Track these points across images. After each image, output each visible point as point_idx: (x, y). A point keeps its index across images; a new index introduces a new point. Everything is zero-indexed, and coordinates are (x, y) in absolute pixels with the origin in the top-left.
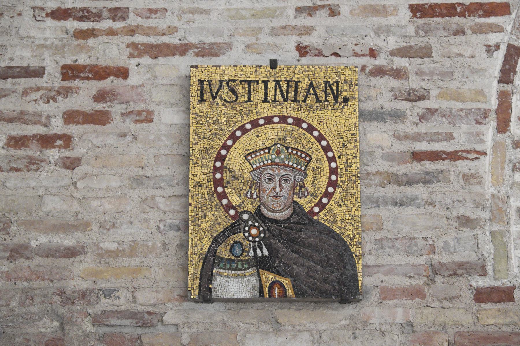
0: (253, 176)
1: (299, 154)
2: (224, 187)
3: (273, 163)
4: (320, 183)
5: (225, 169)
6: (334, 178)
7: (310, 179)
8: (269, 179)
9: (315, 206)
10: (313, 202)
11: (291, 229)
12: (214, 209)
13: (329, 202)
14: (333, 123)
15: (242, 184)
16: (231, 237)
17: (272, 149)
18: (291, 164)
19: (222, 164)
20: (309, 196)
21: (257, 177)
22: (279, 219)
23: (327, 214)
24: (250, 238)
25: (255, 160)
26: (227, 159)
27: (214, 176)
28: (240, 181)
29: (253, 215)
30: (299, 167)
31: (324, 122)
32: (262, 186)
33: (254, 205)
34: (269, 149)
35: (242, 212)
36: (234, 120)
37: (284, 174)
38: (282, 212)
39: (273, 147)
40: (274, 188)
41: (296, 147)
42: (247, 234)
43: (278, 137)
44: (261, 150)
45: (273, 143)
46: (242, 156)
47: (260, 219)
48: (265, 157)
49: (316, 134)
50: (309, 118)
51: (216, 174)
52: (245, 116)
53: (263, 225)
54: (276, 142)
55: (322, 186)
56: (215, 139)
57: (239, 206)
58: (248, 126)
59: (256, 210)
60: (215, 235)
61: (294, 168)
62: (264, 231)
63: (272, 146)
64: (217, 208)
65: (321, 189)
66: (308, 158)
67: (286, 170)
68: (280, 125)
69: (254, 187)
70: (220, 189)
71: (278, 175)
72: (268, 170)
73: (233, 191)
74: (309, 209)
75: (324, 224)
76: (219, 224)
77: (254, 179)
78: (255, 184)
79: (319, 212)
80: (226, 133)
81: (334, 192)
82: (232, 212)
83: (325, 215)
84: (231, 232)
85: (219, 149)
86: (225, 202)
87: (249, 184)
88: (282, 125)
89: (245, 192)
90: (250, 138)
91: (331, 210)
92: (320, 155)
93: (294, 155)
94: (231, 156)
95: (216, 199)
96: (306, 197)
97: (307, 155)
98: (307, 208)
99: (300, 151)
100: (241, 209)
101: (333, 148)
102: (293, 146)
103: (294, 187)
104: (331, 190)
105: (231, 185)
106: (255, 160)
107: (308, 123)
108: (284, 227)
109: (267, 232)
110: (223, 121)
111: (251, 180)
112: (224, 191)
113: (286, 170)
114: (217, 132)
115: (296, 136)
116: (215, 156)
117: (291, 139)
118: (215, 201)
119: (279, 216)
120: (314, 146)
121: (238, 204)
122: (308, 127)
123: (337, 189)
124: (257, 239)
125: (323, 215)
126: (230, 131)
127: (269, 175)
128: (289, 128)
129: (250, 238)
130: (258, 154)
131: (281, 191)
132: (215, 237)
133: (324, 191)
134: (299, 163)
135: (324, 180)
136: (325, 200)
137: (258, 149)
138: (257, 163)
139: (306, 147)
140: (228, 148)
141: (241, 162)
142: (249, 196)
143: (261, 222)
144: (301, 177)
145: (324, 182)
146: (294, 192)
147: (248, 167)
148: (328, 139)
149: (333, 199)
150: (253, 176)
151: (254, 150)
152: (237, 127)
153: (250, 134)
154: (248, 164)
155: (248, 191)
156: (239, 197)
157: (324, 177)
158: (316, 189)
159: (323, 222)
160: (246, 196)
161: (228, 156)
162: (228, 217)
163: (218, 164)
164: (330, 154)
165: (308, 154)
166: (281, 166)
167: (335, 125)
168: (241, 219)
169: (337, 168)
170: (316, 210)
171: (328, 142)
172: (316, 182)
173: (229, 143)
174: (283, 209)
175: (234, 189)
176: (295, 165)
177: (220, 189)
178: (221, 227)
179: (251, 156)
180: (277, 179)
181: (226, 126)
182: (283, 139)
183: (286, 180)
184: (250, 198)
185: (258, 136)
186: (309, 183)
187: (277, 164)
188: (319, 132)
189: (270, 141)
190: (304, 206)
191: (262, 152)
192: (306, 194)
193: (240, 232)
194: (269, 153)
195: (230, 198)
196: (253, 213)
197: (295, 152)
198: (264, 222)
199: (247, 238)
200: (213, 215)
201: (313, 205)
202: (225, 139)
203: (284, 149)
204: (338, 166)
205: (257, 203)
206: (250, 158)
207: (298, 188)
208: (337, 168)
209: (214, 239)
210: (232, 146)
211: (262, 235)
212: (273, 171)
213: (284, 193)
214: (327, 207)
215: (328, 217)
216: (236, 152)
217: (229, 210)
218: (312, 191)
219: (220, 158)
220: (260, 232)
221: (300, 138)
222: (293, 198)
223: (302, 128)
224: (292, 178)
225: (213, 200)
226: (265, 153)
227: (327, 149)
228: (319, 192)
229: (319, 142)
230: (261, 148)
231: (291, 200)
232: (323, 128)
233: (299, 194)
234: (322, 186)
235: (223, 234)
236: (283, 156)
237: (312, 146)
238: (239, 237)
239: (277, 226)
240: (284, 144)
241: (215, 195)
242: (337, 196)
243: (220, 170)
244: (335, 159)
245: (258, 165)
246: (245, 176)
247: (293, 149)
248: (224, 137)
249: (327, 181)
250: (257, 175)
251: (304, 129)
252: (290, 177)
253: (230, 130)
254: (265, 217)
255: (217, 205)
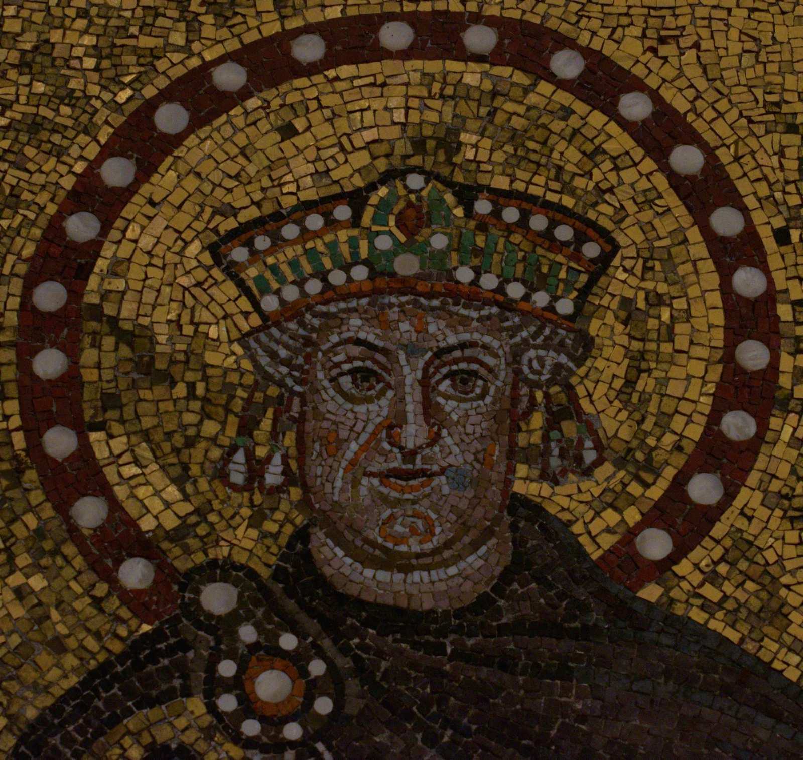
0: (264, 360)
1: (538, 222)
2: (82, 429)
3: (381, 283)
4: (674, 389)
5: (93, 325)
6: (753, 355)
7: (609, 363)
8: (362, 375)
9: (648, 521)
10: (633, 501)
11: (503, 667)
12: (23, 560)
13: (729, 496)
14: (735, 48)
15: (196, 405)
16: (131, 723)
17: (374, 199)
18: (489, 282)
19: (75, 293)
20: (607, 468)
21: (287, 363)
22: (427, 604)
23: (723, 569)
24: (251, 728)
25: (274, 269)
26: (101, 264)
27: (24, 364)
28: (181, 390)
29: (262, 587)
30: (541, 299)
31: (685, 42)
32: (319, 416)
33: (271, 527)
34: (357, 199)
35: (199, 569)
36: (146, 42)
37: (452, 340)
38: (445, 564)
39: (383, 191)
40: (393, 425)
41: (520, 186)
42: (228, 703)
43: (410, 132)
44: (308, 206)
45: (382, 165)
46: (194, 249)
47: (312, 613)
48: (333, 246)
49: (635, 107)
50: (595, 24)
51: (35, 352)
52: (209, 19)
53: (326, 643)
54: (396, 161)
55: (685, 407)
56: (30, 152)
57: (177, 535)
58: (230, 77)
59: (283, 558)
60: (31, 713)
61: (508, 306)
62: (334, 683)
63: (372, 187)
64: (43, 552)
65: (678, 423)
66: (592, 247)
67: (465, 321)
68: (418, 64)
69: (266, 424)
70: (59, 442)
71: (412, 350)
72: (355, 321)
73: (143, 450)
74: (607, 541)
75: (702, 631)
76: (58, 646)
77: (268, 377)
78: (278, 403)
79: (674, 558)
80: (99, 119)
81: (760, 438)
82: (135, 573)
83: (712, 578)
84: (128, 692)
85: (52, 209)
86: (89, 512)
87: (238, 405)
88: (433, 66)
89: (216, 453)
90: (241, 140)
91: (742, 547)
92: (664, 226)
93: (509, 229)
94: (125, 250)
95: (36, 497)
96: (587, 472)
97: (587, 229)
98: (597, 534)
99: (547, 206)
100: (188, 551)
101: (743, 186)
102: (501, 182)
103: (511, 417)
104: (738, 425)
105: (128, 413)
106: (274, 269)
107: (587, 52)
108: (459, 655)
109: (353, 686)
110: (78, 52)
111: (249, 380)
112: (85, 450)
113: (465, 321)
114: (44, 111)
115: (518, 123)
116: (29, 250)
117: (487, 143)
118: (30, 509)
119: (424, 589)
120: (629, 175)
121: (170, 522)
122: (589, 70)
123: (774, 423)
124: (292, 732)
125: (697, 578)
126: (118, 108)
127: (356, 350)
128: (471, 79)
129: (251, 728)
130: (290, 231)
131: (435, 439)
132: (32, 726)
133: (695, 432)
134: (544, 277)
135: (697, 368)
136: (703, 489)
137: (289, 202)
138: (282, 281)
139: (580, 182)
140: (107, 204)
141: (185, 281)
142: (238, 478)
143: (312, 625)
144: (551, 357)
145: (696, 384)
146: (513, 444)
147: (231, 308)
148: (708, 137)
149: (753, 478)
150: (264, 360)
151: (268, 208)
152: (162, 83)
153: (240, 122)
154: (231, 289)
155: (234, 449)
156: (179, 482)
157: (697, 351)
158: (648, 425)
159: (697, 616)
160: (222, 475)
161: (108, 250)
162: (114, 603)
163: (50, 296)
164: (726, 222)
165: (593, 225)
166: (430, 296)
167: (748, 60)
168: (194, 611)
169: (771, 296)
170: (656, 545)
171: (709, 152)
172: (645, 383)
173: (117, 172)
174: (447, 545)
175: (146, 436)
176: (515, 291)
177: (59, 442)
178: (70, 661)
179: (249, 244)
180: (410, 374)
181: (95, 77)
182: (441, 143)
183: (463, 380)
184: (248, 487)
185: (288, 132)
186: (602, 388)
187: (405, 286)
188: (655, 96)
189: (361, 159)
190: (577, 528)
191: (315, 221)
192: (590, 456)
193: (187, 693)
194: (355, 221)
195: (121, 492)
196: (265, 573)
197: (511, 215)
198: (330, 627)
199: (225, 727)
200: (20, 593)
201: (633, 516)
202: (92, 151)
203: (449, 198)
204: (780, 284)
205: (285, 517)
206: (240, 254)
207: (537, 420)
208: (771, 296)
209: (21, 740)
210: (130, 191)
211: (324, 706)
212: (387, 326)
213: (453, 452)
214: (719, 530)
215: (728, 588)
216: (159, 224)
217: (119, 562)
218: (625, 433)
219: (66, 261)
220: (313, 689)
221: (539, 134)
222: (508, 483)
223: (551, 77)
224: (499, 364)
225: (19, 507)
226: (331, 223)
227: (706, 191)
228: (669, 440)
229: (659, 153)
230: (304, 196)
231: (494, 494)
232: (681, 74)
233: (546, 453)
234: (685, 407)
235: (82, 708)
236: (439, 242)
237: (613, 178)
238: (181, 723)
239: (415, 645)
240: (445, 171)
241: (31, 476)
242: (778, 458)
243: (61, 328)
244: (759, 246)
245: (291, 293)
246: (211, 358)
247: (500, 197)
248: (83, 139)
249: (716, 373)
250: (283, 353)
251: (561, 84)
252: (490, 361)
253: (123, 96)
254: (343, 599)
255: (40, 534)
